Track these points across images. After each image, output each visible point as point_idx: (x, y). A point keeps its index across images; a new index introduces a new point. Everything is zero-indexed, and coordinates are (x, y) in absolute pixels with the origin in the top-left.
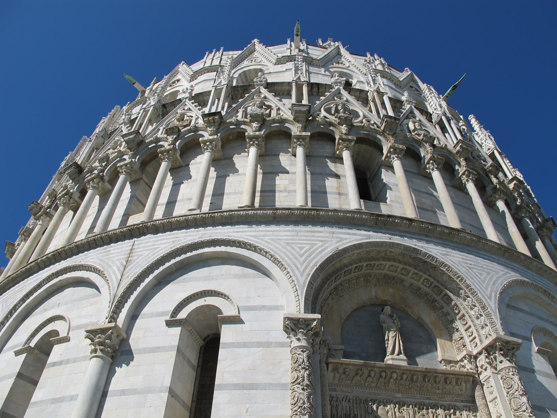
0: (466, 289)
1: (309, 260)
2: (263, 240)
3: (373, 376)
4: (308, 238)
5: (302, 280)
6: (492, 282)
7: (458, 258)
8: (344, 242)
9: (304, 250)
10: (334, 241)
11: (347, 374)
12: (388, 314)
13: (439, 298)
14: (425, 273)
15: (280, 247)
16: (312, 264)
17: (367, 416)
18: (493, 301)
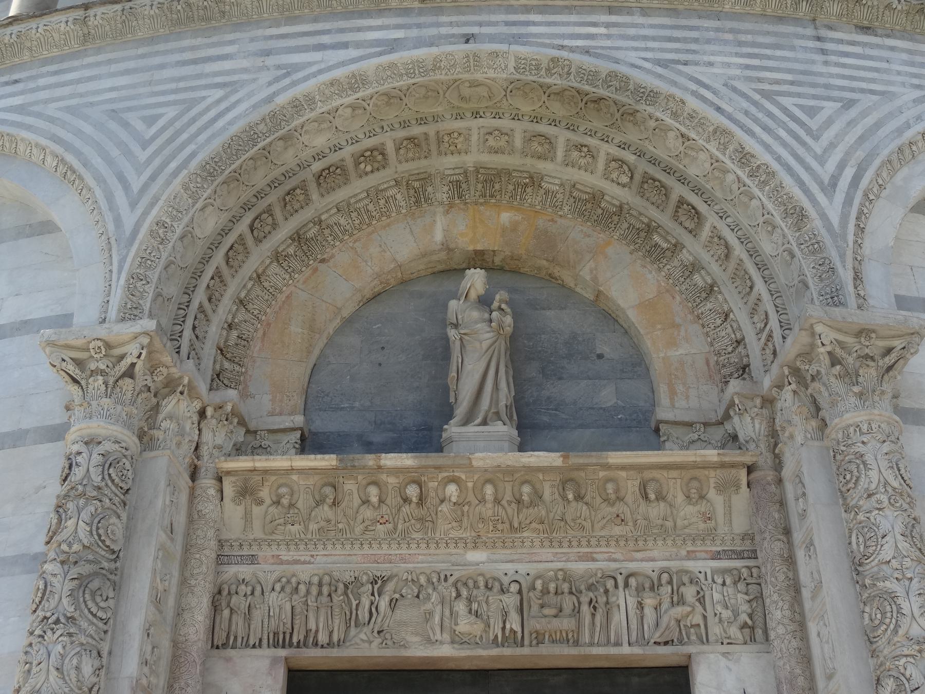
0: (739, 172)
1: (167, 152)
2: (39, 115)
3: (374, 500)
4: (182, 85)
5: (129, 221)
6: (859, 130)
7: (728, 65)
8: (300, 75)
9: (161, 123)
10: (265, 77)
11: (285, 501)
12: (473, 295)
13: (664, 219)
14: (605, 139)
15: (88, 129)
16: (173, 165)
17: (353, 631)
18: (840, 196)
